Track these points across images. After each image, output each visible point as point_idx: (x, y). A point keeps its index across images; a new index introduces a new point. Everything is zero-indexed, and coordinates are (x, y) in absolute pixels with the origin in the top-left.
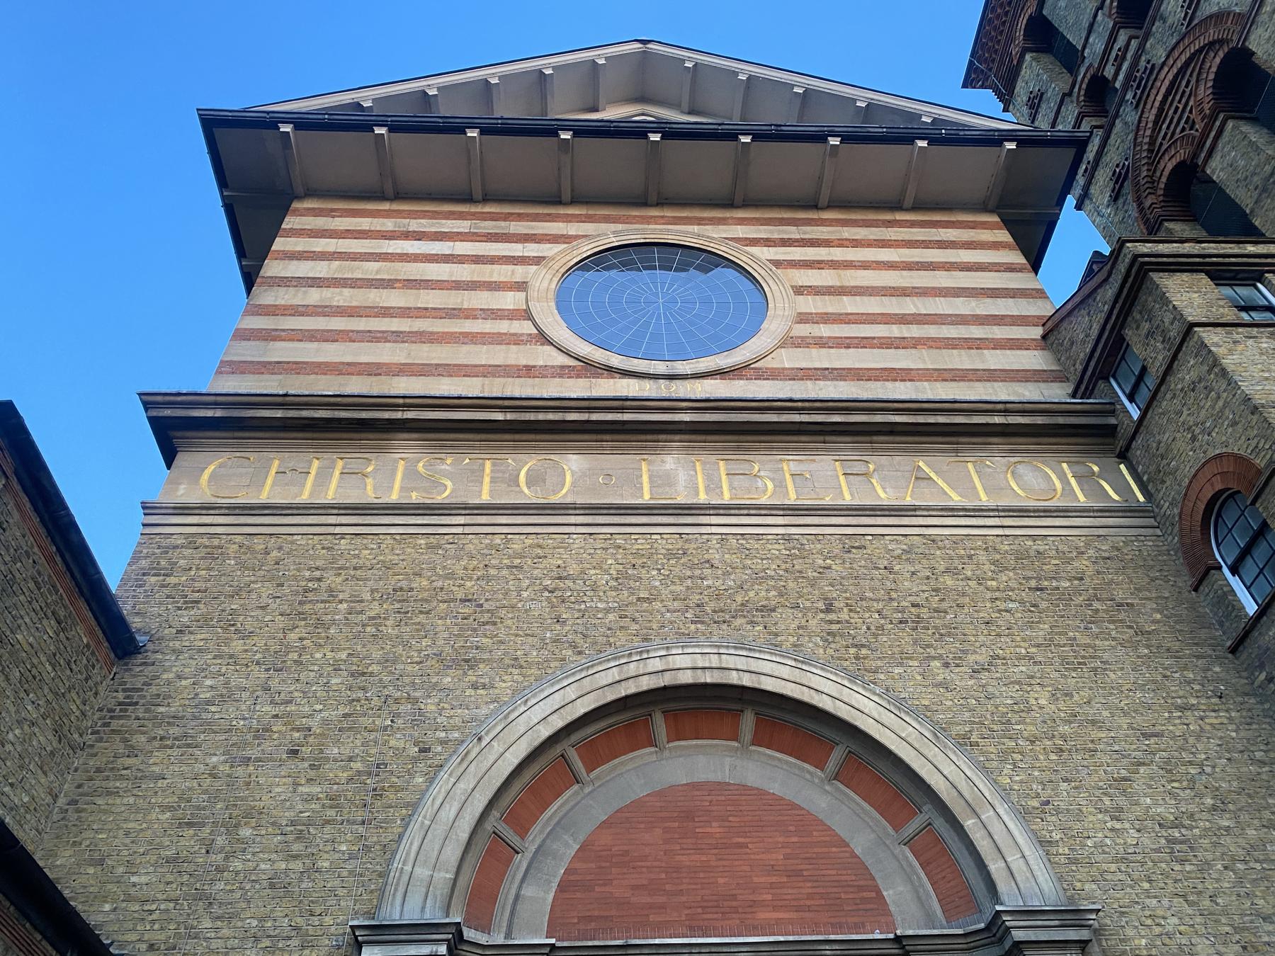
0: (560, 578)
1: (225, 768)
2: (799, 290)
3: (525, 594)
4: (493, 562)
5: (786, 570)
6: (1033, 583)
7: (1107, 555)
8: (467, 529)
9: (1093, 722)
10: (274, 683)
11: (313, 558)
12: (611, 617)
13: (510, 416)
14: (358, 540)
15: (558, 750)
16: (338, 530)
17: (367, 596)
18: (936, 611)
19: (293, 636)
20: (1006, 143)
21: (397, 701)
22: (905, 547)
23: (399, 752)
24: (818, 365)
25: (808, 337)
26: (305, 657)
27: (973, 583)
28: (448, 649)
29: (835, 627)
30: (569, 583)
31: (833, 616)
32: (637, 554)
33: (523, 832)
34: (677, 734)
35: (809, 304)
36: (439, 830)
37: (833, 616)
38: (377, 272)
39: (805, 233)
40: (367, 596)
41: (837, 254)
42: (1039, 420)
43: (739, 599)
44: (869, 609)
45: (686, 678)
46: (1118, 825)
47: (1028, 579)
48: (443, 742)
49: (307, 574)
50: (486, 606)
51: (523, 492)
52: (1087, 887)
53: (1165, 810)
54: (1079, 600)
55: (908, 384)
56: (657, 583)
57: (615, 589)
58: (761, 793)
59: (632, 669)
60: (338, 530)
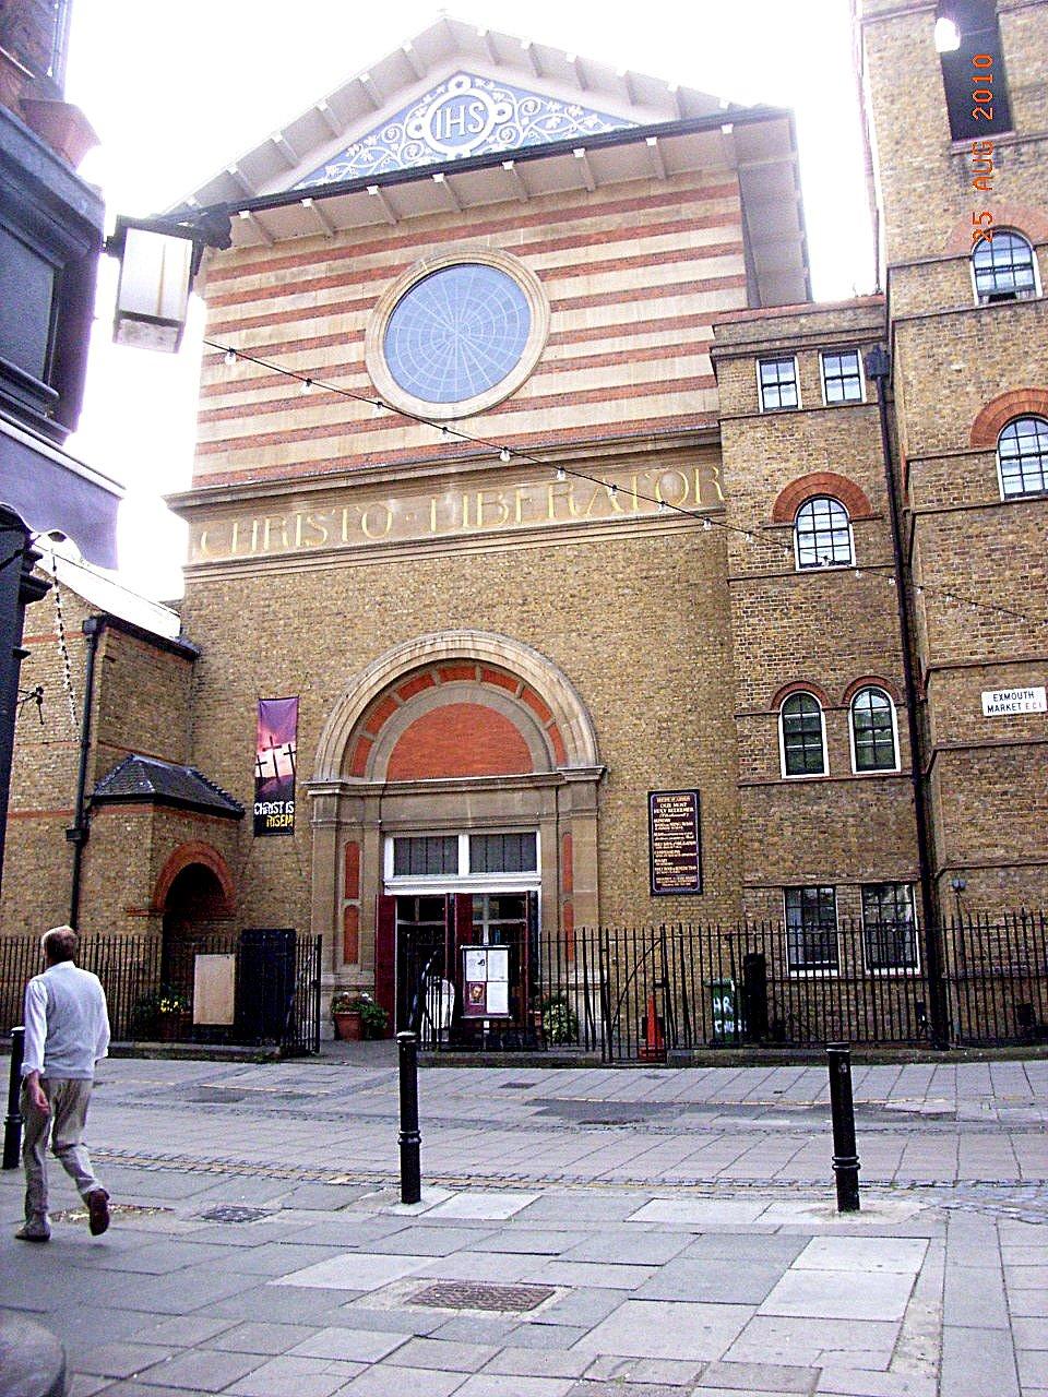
0: (385, 595)
1: (246, 714)
2: (555, 306)
3: (367, 607)
4: (351, 587)
5: (506, 578)
6: (644, 574)
7: (695, 547)
8: (337, 565)
9: (646, 666)
10: (258, 670)
11: (264, 592)
12: (410, 618)
13: (350, 483)
14: (284, 579)
15: (386, 694)
16: (273, 572)
17: (292, 615)
18: (584, 598)
19: (262, 641)
20: (723, 127)
21: (311, 675)
22: (576, 553)
23: (315, 702)
24: (554, 392)
25: (552, 361)
26: (269, 654)
27: (609, 577)
28: (331, 645)
29: (525, 615)
30: (389, 598)
31: (525, 608)
32: (425, 574)
33: (375, 733)
34: (445, 678)
35: (564, 322)
36: (333, 740)
37: (525, 608)
38: (270, 337)
39: (573, 229)
40: (292, 615)
41: (595, 253)
42: (677, 444)
43: (477, 601)
44: (546, 601)
45: (443, 656)
46: (638, 722)
47: (642, 570)
48: (333, 696)
49: (262, 603)
50: (349, 616)
51: (363, 533)
52: (613, 753)
53: (664, 714)
54: (668, 583)
55: (613, 402)
56: (434, 594)
57: (412, 600)
58: (482, 707)
59: (417, 653)
60: (273, 572)
